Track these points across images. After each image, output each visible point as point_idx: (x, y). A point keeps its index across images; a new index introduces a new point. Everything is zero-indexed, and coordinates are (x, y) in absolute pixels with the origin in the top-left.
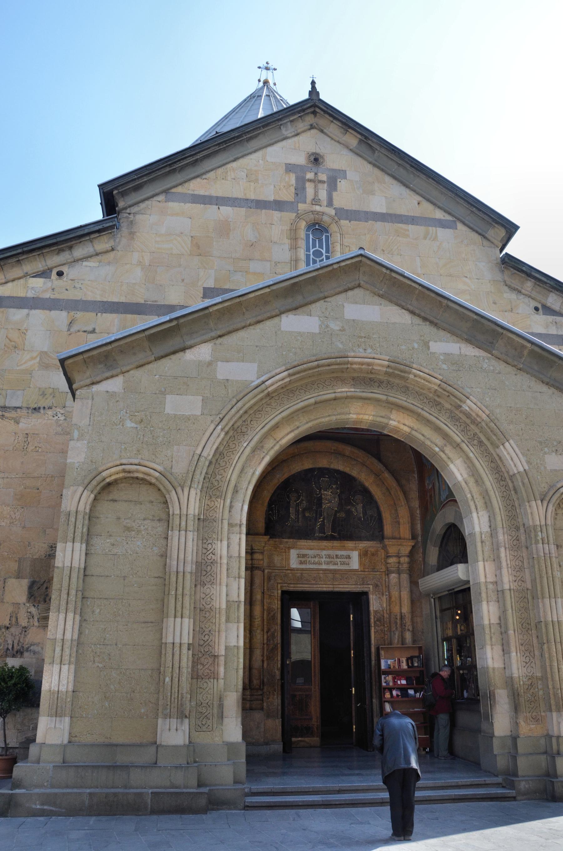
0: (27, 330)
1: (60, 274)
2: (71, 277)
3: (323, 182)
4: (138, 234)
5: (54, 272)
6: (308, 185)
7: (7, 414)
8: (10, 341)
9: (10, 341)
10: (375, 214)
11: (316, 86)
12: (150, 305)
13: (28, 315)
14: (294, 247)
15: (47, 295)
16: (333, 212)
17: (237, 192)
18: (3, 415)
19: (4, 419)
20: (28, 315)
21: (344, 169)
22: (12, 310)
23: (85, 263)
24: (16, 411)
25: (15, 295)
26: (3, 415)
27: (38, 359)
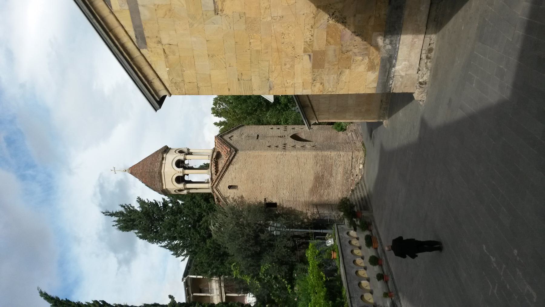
0: (155, 5)
7: (220, 8)
8: (166, 14)
9: (166, 14)
13: (143, 6)
18: (221, 10)
19: (223, 9)
20: (143, 6)
22: (142, 17)
24: (217, 2)
26: (221, 10)
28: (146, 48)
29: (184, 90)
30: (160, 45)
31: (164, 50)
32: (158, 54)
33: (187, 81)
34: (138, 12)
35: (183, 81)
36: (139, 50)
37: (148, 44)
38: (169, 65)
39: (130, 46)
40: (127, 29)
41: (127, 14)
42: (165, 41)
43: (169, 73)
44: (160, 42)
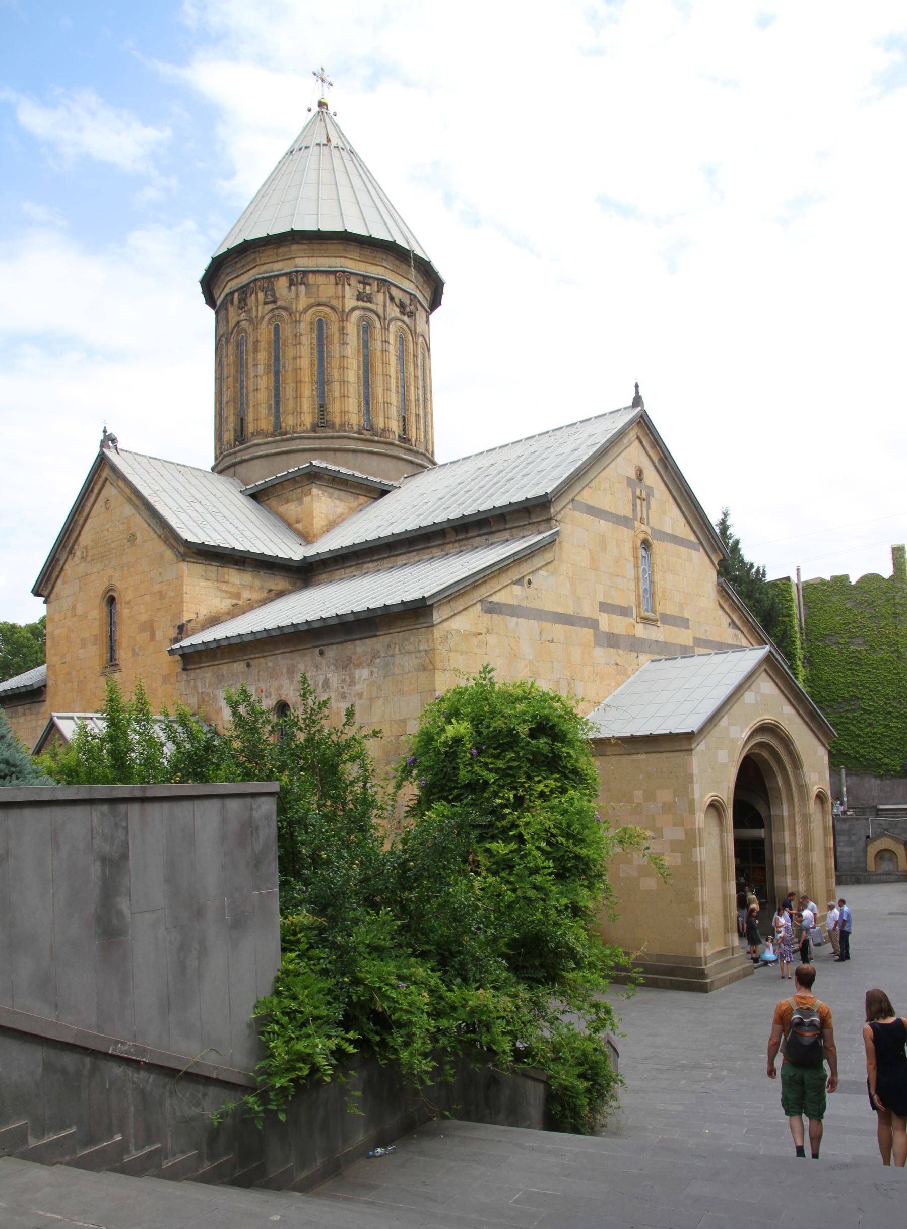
1: (529, 582)
2: (535, 587)
3: (644, 500)
4: (563, 544)
5: (526, 580)
6: (638, 501)
10: (668, 534)
11: (640, 389)
12: (577, 617)
14: (636, 566)
15: (524, 604)
16: (649, 531)
17: (604, 502)
21: (652, 486)
22: (508, 618)
23: (541, 572)
25: (506, 602)
27: (528, 669)
28: (482, 610)
29: (440, 647)
30: (485, 631)
31: (481, 634)
32: (477, 624)
33: (451, 654)
34: (512, 615)
35: (450, 650)
36: (480, 601)
37: (485, 614)
38: (466, 636)
39: (483, 591)
40: (498, 594)
41: (511, 601)
42: (492, 639)
43: (458, 631)
44: (488, 632)
